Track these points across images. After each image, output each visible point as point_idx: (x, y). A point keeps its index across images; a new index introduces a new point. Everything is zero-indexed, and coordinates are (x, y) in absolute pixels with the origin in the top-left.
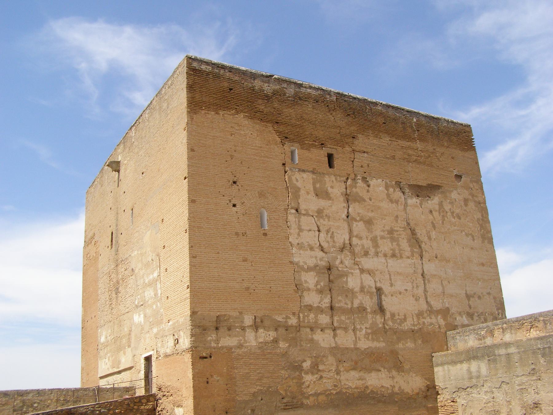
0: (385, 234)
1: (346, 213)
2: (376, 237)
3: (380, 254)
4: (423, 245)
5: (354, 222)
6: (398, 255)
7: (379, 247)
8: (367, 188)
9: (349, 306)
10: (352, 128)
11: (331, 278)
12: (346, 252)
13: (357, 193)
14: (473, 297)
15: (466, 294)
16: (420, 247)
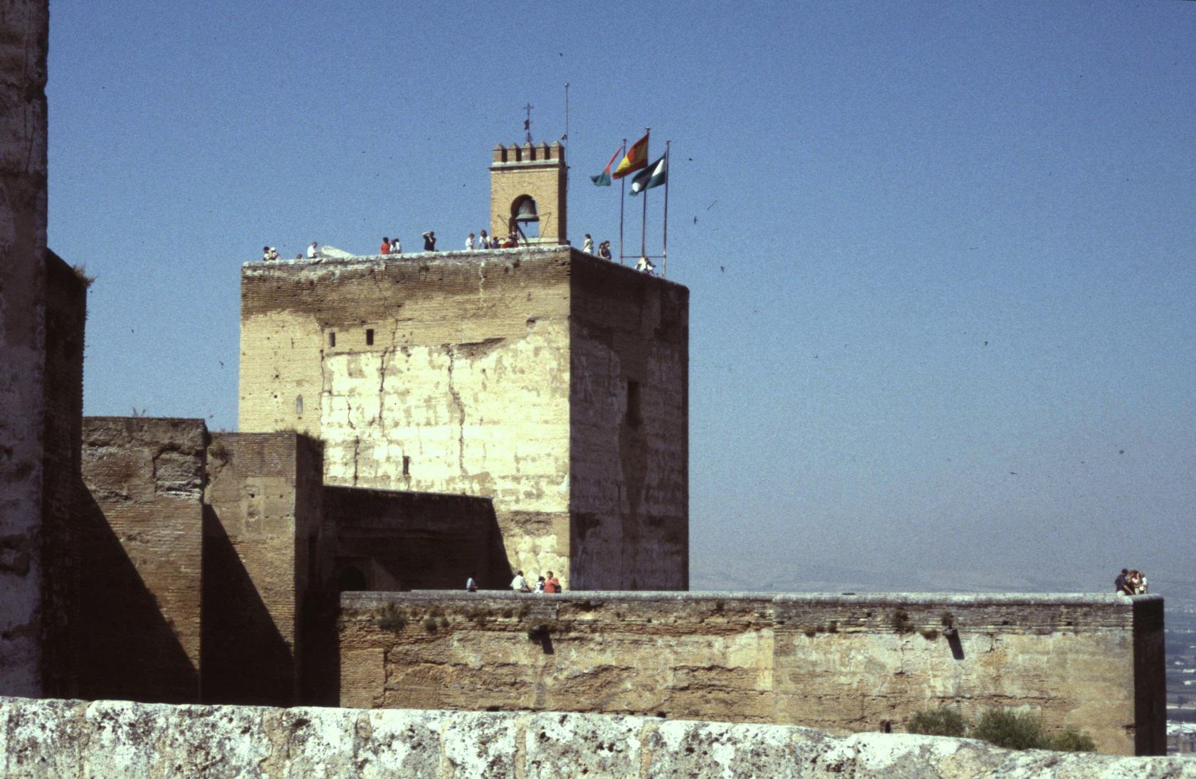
0: (422, 403)
1: (379, 388)
2: (410, 407)
3: (412, 424)
4: (467, 410)
5: (387, 397)
6: (433, 422)
7: (411, 417)
8: (406, 358)
9: (373, 475)
10: (401, 295)
11: (358, 451)
12: (375, 425)
13: (394, 366)
14: (525, 459)
15: (516, 456)
16: (462, 411)
